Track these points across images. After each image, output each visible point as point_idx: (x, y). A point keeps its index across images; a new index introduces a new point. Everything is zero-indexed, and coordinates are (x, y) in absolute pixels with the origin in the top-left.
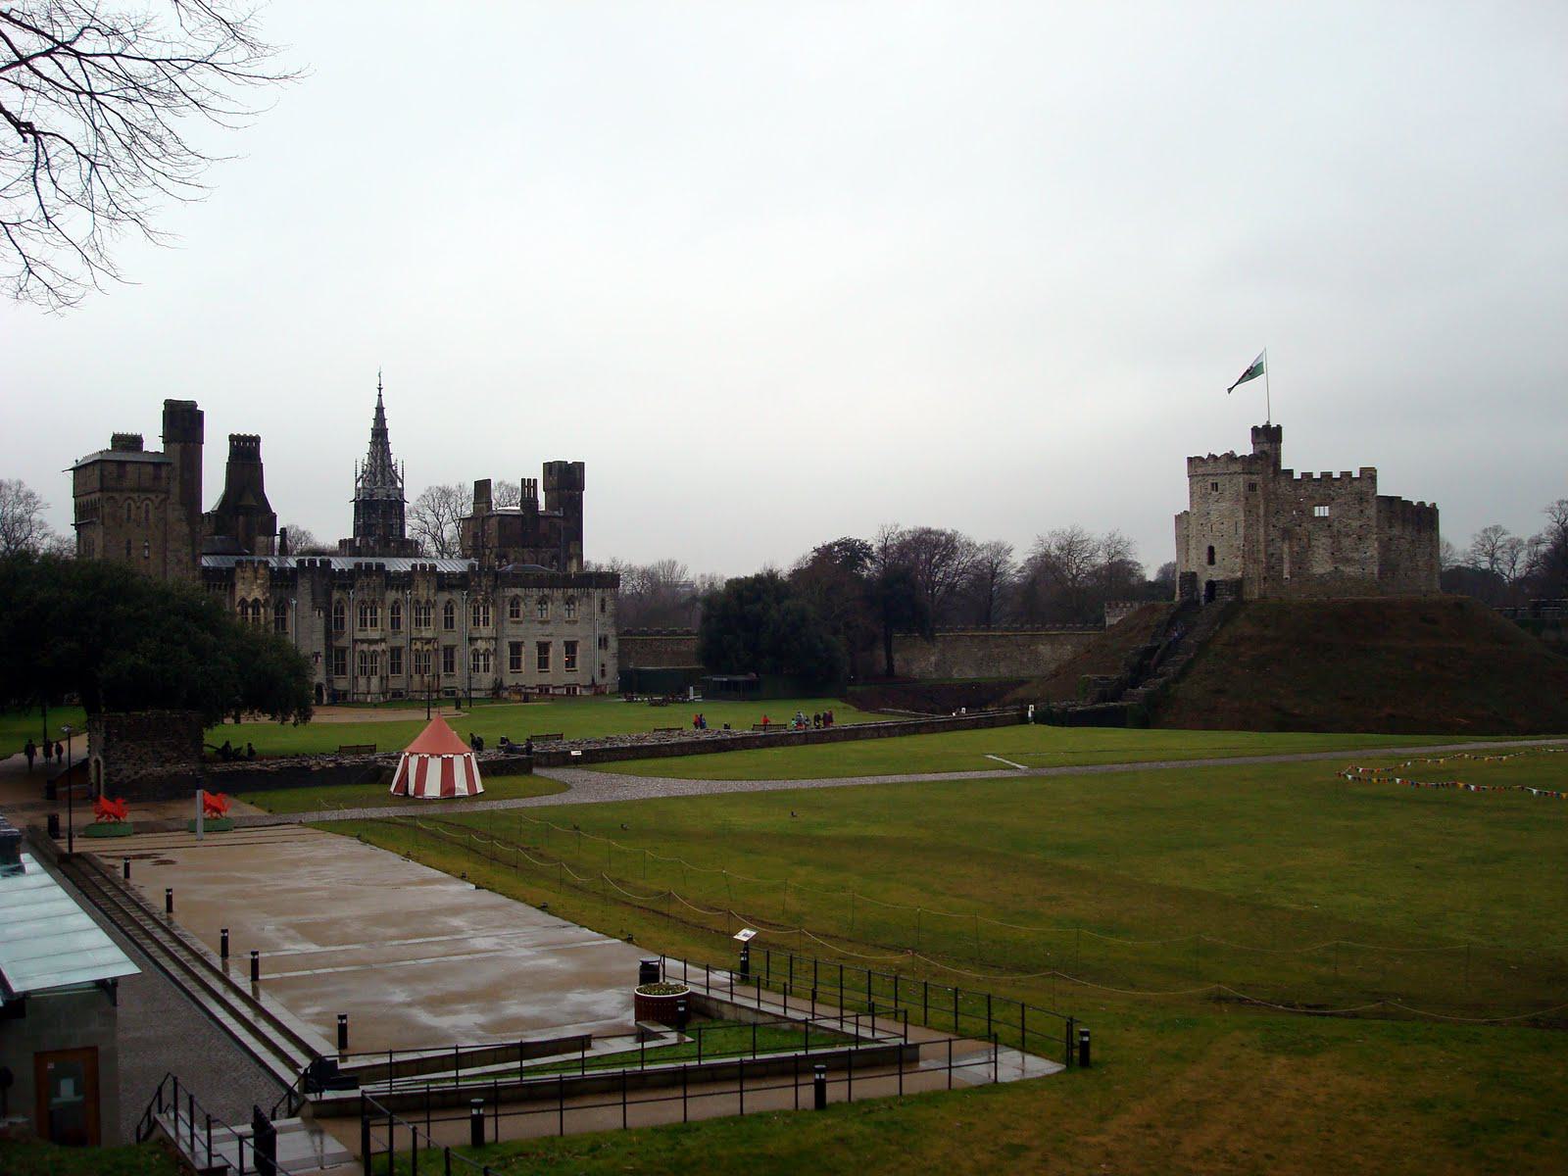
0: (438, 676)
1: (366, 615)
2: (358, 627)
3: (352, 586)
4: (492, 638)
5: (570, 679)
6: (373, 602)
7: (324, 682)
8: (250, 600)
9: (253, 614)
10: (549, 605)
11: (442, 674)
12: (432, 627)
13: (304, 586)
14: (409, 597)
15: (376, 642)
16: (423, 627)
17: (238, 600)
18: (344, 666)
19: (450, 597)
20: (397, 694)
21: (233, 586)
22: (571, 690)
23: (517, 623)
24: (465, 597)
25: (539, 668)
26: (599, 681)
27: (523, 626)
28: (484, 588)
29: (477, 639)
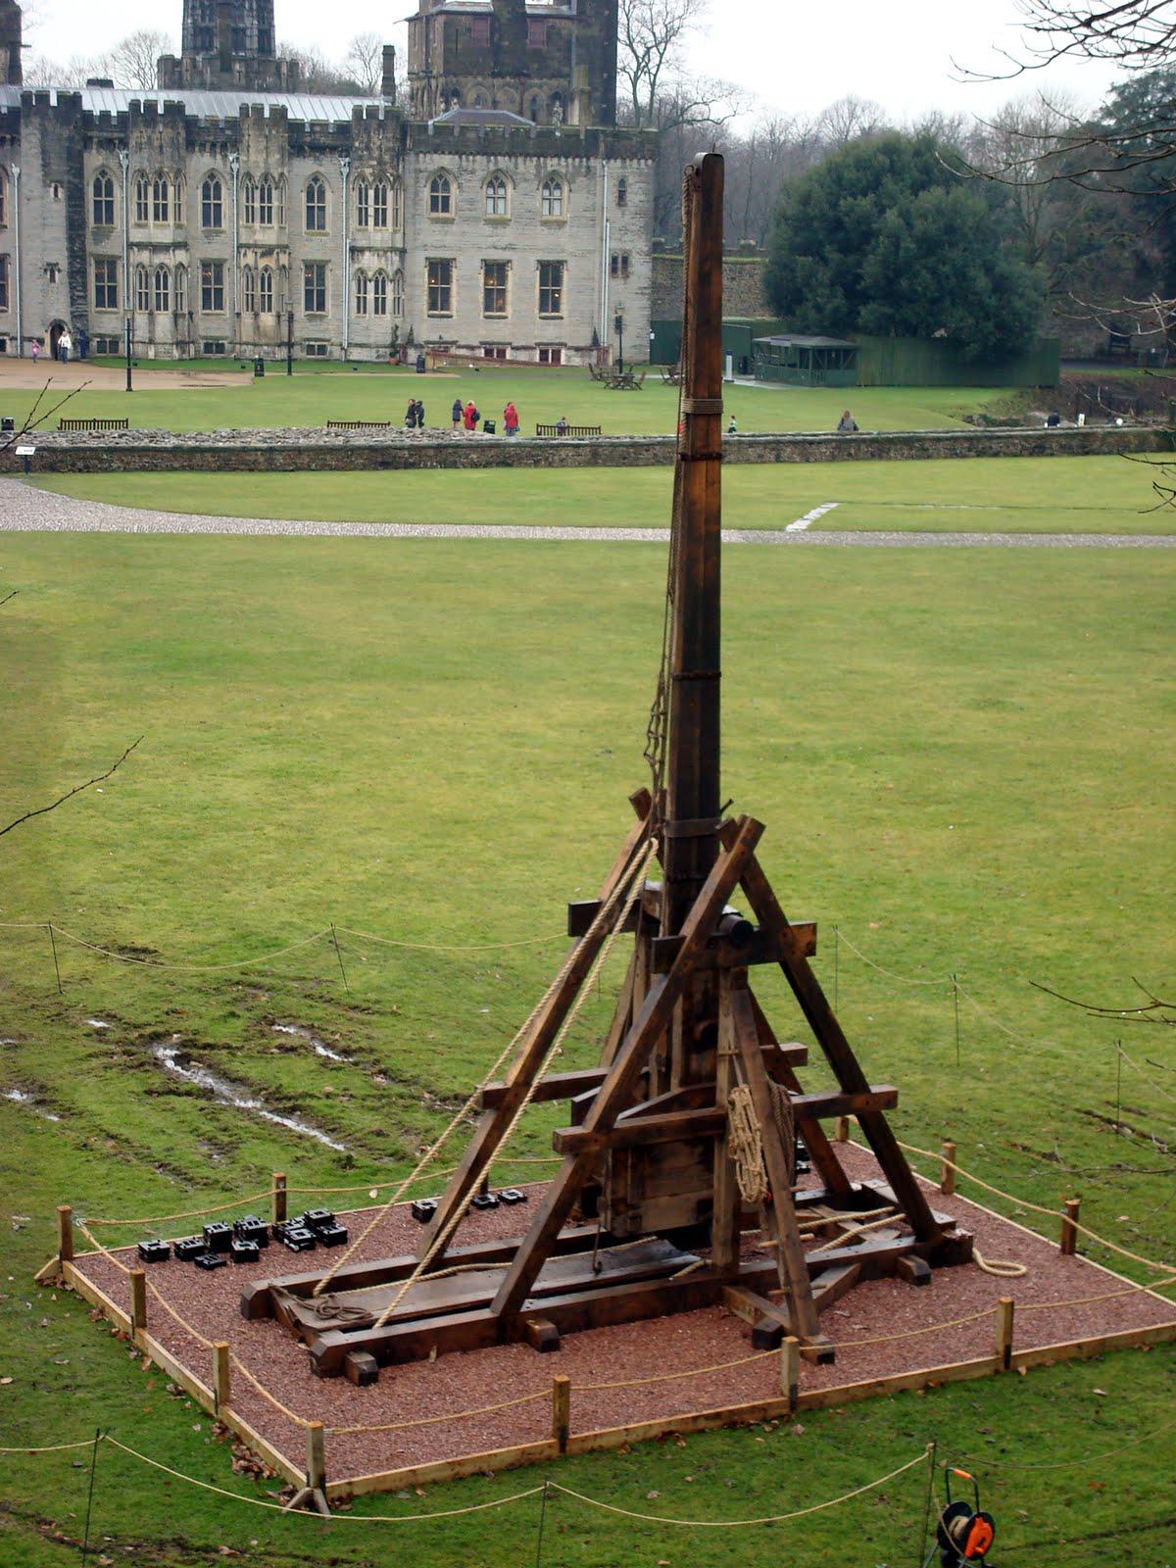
1: (146, 198)
2: (133, 219)
3: (124, 143)
4: (393, 249)
5: (549, 333)
6: (160, 174)
7: (66, 318)
10: (509, 188)
11: (300, 312)
13: (30, 138)
14: (235, 166)
16: (257, 224)
18: (113, 290)
20: (214, 347)
22: (549, 355)
24: (345, 170)
25: (487, 308)
26: (607, 337)
27: (454, 228)
28: (376, 154)
29: (362, 250)
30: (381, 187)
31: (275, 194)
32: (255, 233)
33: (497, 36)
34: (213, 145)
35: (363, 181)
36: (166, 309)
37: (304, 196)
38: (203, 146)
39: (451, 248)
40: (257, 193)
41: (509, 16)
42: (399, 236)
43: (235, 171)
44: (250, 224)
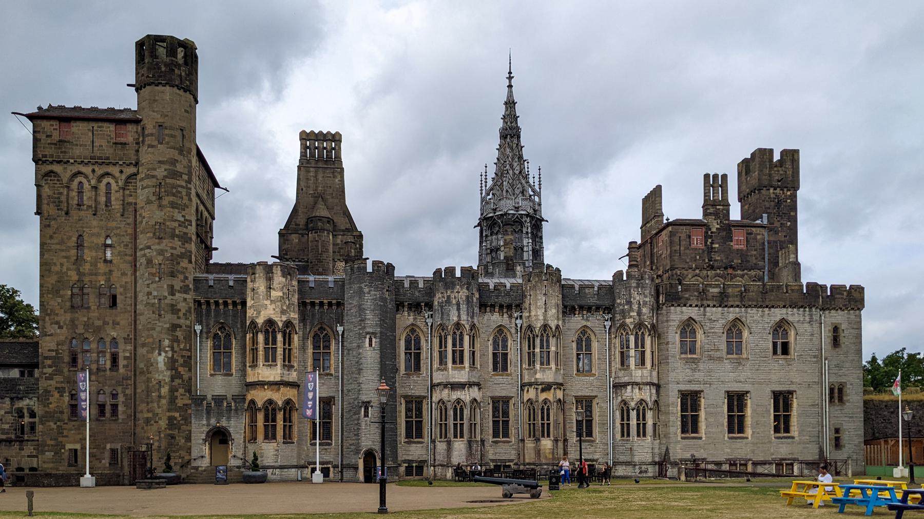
0: (565, 440)
2: (436, 365)
4: (653, 384)
7: (377, 447)
8: (260, 321)
9: (266, 343)
12: (553, 366)
15: (461, 386)
16: (538, 366)
17: (248, 324)
18: (419, 424)
19: (584, 323)
21: (244, 303)
23: (694, 361)
24: (608, 324)
27: (701, 366)
28: (635, 307)
29: (625, 385)
30: (640, 333)
31: (553, 341)
32: (536, 373)
33: (710, 240)
34: (501, 306)
35: (624, 330)
36: (462, 437)
37: (574, 345)
38: (493, 306)
39: (699, 382)
40: (538, 341)
41: (718, 226)
42: (655, 373)
43: (519, 326)
44: (532, 367)
